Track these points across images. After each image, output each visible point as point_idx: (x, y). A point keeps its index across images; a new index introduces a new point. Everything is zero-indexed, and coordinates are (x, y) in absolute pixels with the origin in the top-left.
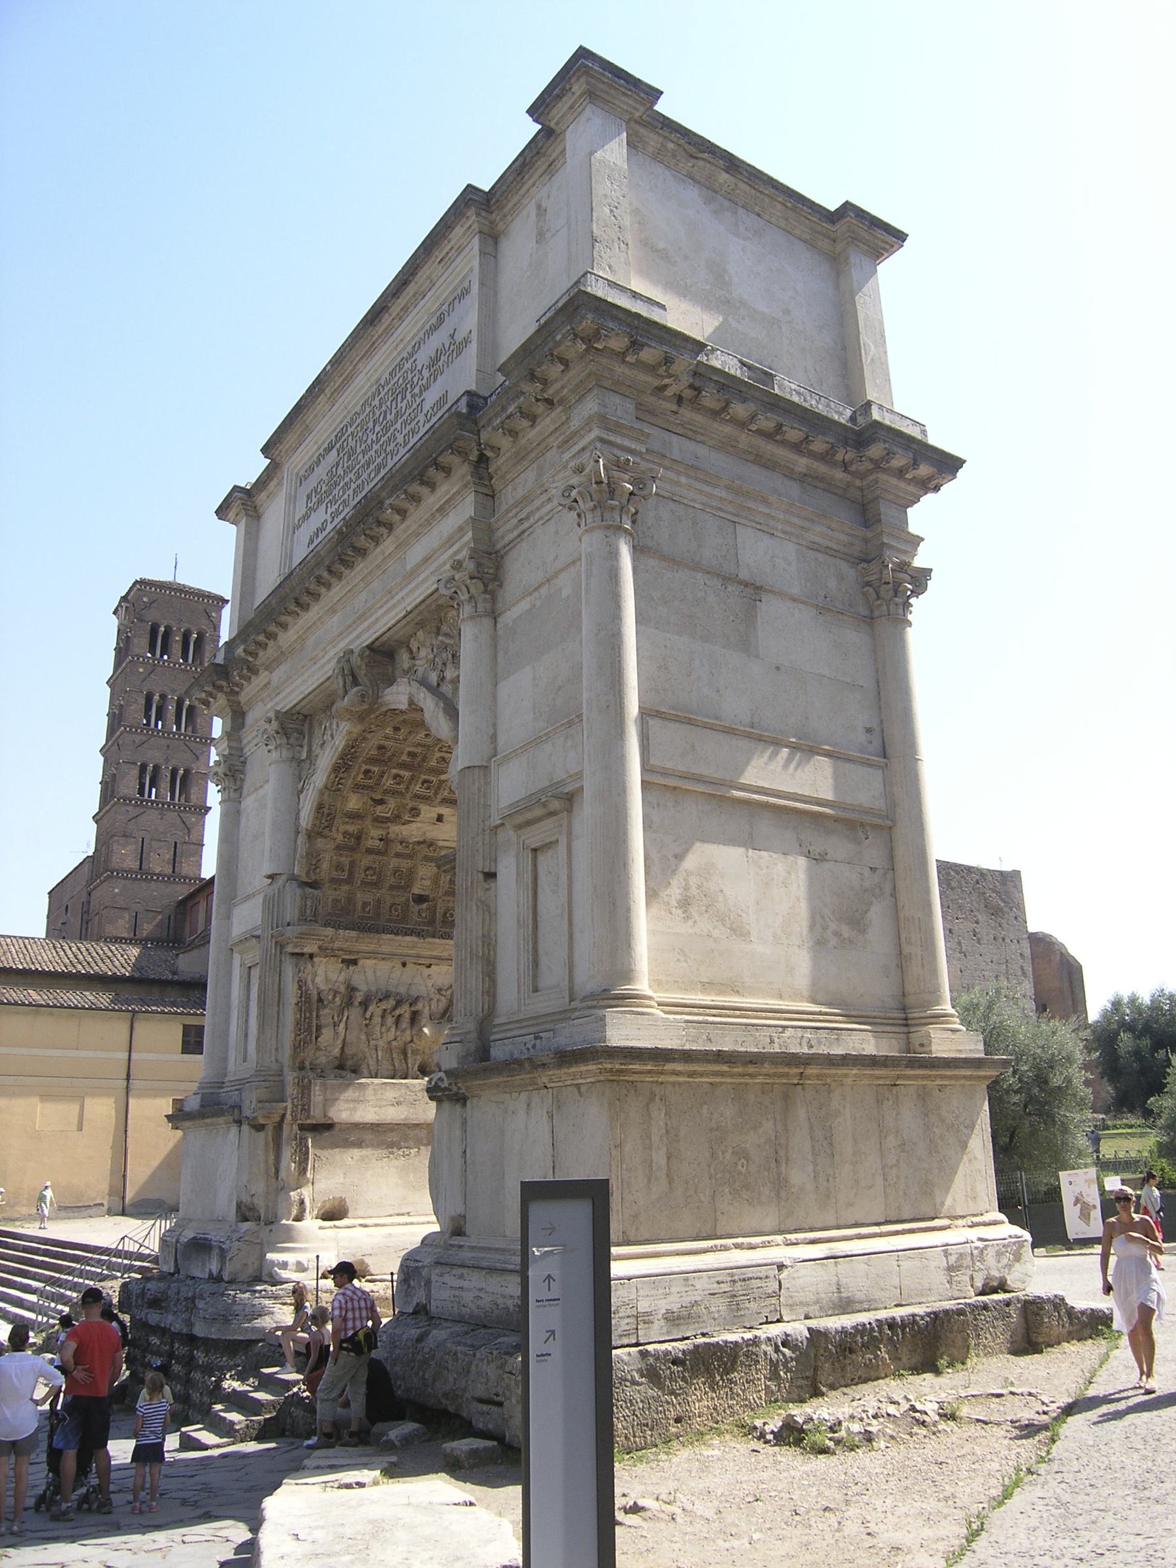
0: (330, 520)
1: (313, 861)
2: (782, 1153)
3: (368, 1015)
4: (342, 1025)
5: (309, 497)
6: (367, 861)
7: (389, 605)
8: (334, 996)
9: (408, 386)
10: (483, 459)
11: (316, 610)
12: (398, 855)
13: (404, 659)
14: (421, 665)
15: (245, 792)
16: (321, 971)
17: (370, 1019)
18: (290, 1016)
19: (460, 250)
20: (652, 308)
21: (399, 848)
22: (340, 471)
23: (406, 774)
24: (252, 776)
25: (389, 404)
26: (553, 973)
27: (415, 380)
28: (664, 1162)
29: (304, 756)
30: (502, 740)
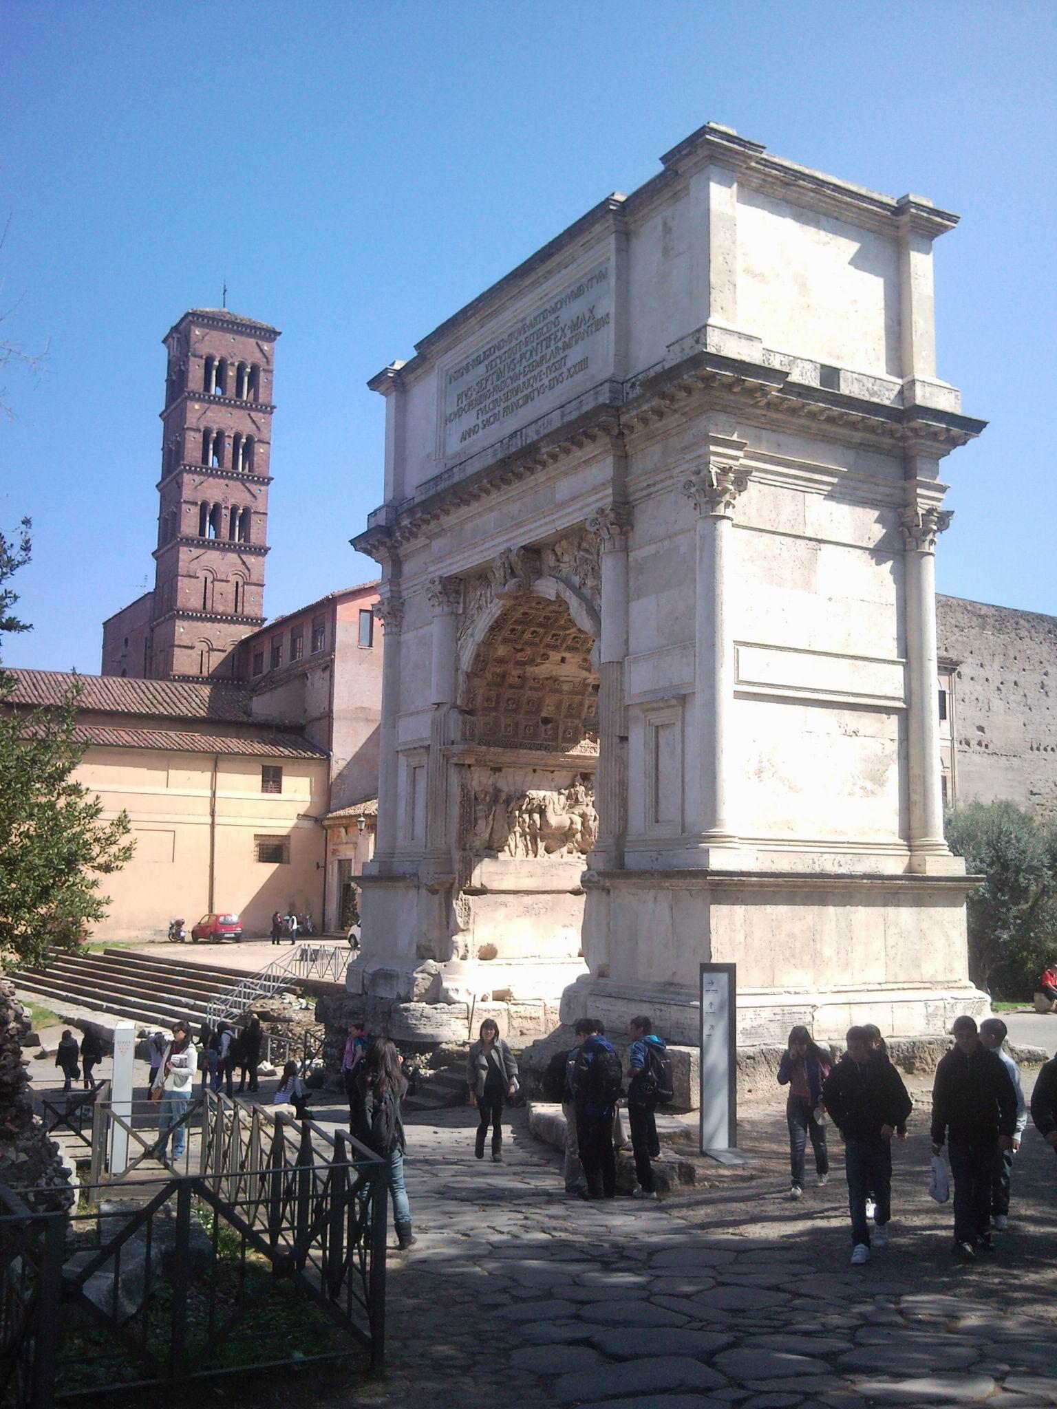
0: (481, 426)
1: (470, 693)
2: (817, 936)
3: (510, 809)
4: (491, 817)
5: (460, 397)
6: (508, 693)
7: (542, 522)
8: (485, 796)
9: (553, 337)
10: (621, 434)
11: (475, 507)
12: (530, 689)
13: (550, 560)
14: (565, 569)
15: (404, 629)
16: (476, 777)
17: (511, 812)
18: (455, 811)
19: (599, 241)
20: (751, 343)
21: (532, 683)
22: (490, 387)
23: (541, 630)
24: (410, 618)
25: (534, 344)
26: (669, 809)
27: (559, 334)
28: (742, 939)
29: (461, 611)
30: (632, 643)
